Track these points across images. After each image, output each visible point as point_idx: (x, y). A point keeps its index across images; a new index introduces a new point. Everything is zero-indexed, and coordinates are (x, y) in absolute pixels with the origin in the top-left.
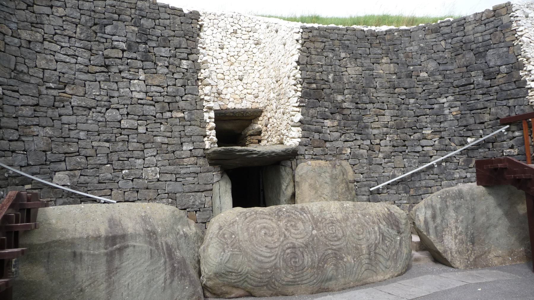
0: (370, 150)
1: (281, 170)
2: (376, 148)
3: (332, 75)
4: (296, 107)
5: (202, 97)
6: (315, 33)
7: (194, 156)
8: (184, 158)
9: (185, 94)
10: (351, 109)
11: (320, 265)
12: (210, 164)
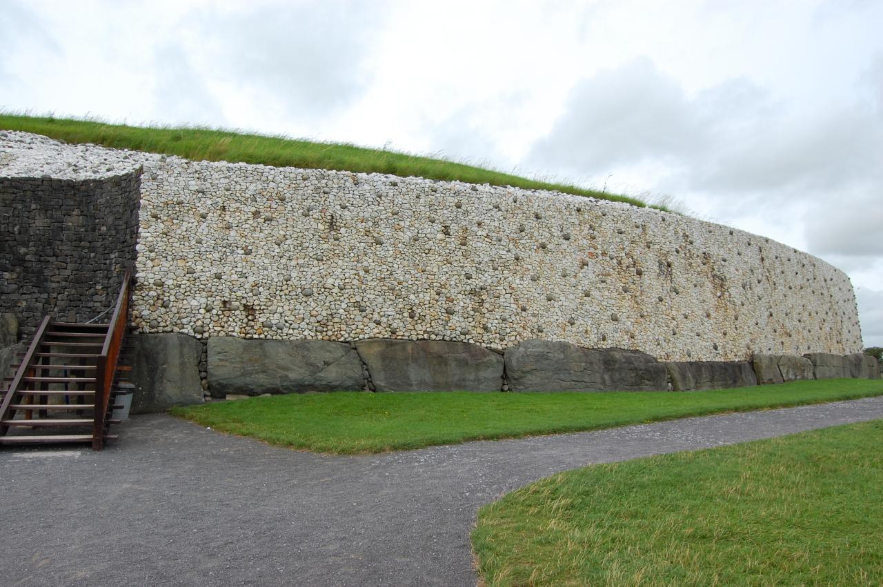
0: (46, 303)
2: (53, 301)
3: (18, 227)
6: (6, 183)
10: (32, 261)
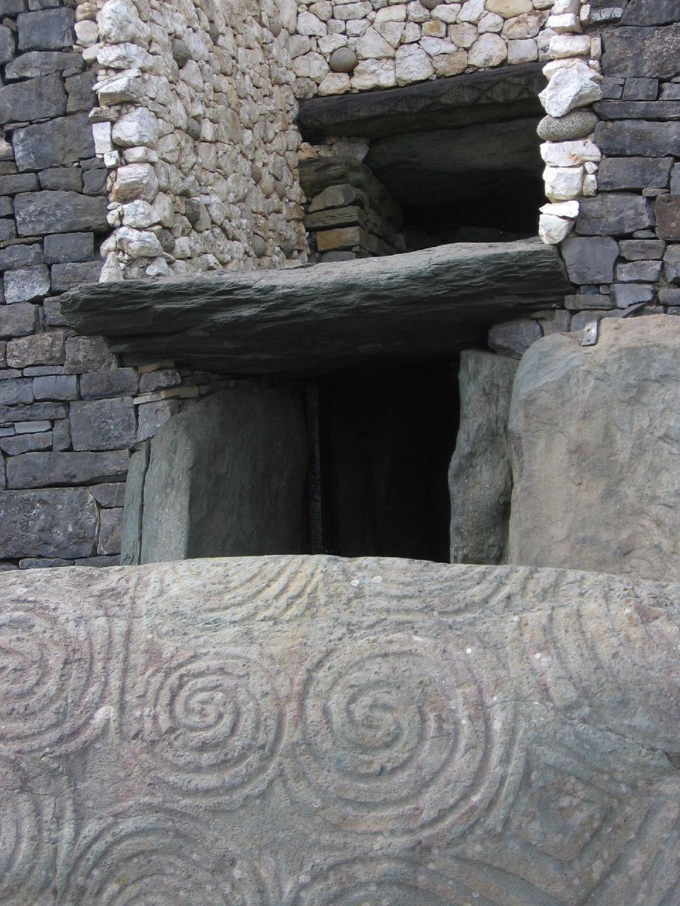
1: (463, 376)
4: (573, 33)
5: (87, 55)
7: (53, 327)
8: (9, 338)
9: (18, 53)
11: (80, 880)
12: (122, 360)
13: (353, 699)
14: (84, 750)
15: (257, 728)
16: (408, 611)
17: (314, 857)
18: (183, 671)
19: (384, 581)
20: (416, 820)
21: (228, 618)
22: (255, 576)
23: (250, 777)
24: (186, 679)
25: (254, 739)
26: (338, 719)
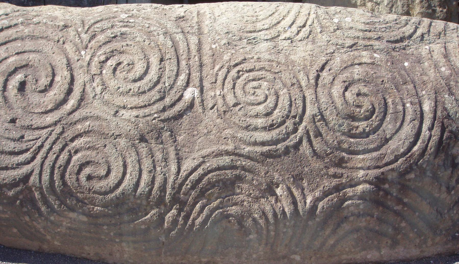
13: (346, 89)
14: (179, 116)
15: (291, 105)
16: (369, 39)
17: (324, 181)
18: (238, 68)
19: (353, 21)
20: (382, 161)
21: (262, 37)
22: (273, 13)
23: (288, 135)
24: (241, 73)
25: (290, 112)
26: (339, 102)
